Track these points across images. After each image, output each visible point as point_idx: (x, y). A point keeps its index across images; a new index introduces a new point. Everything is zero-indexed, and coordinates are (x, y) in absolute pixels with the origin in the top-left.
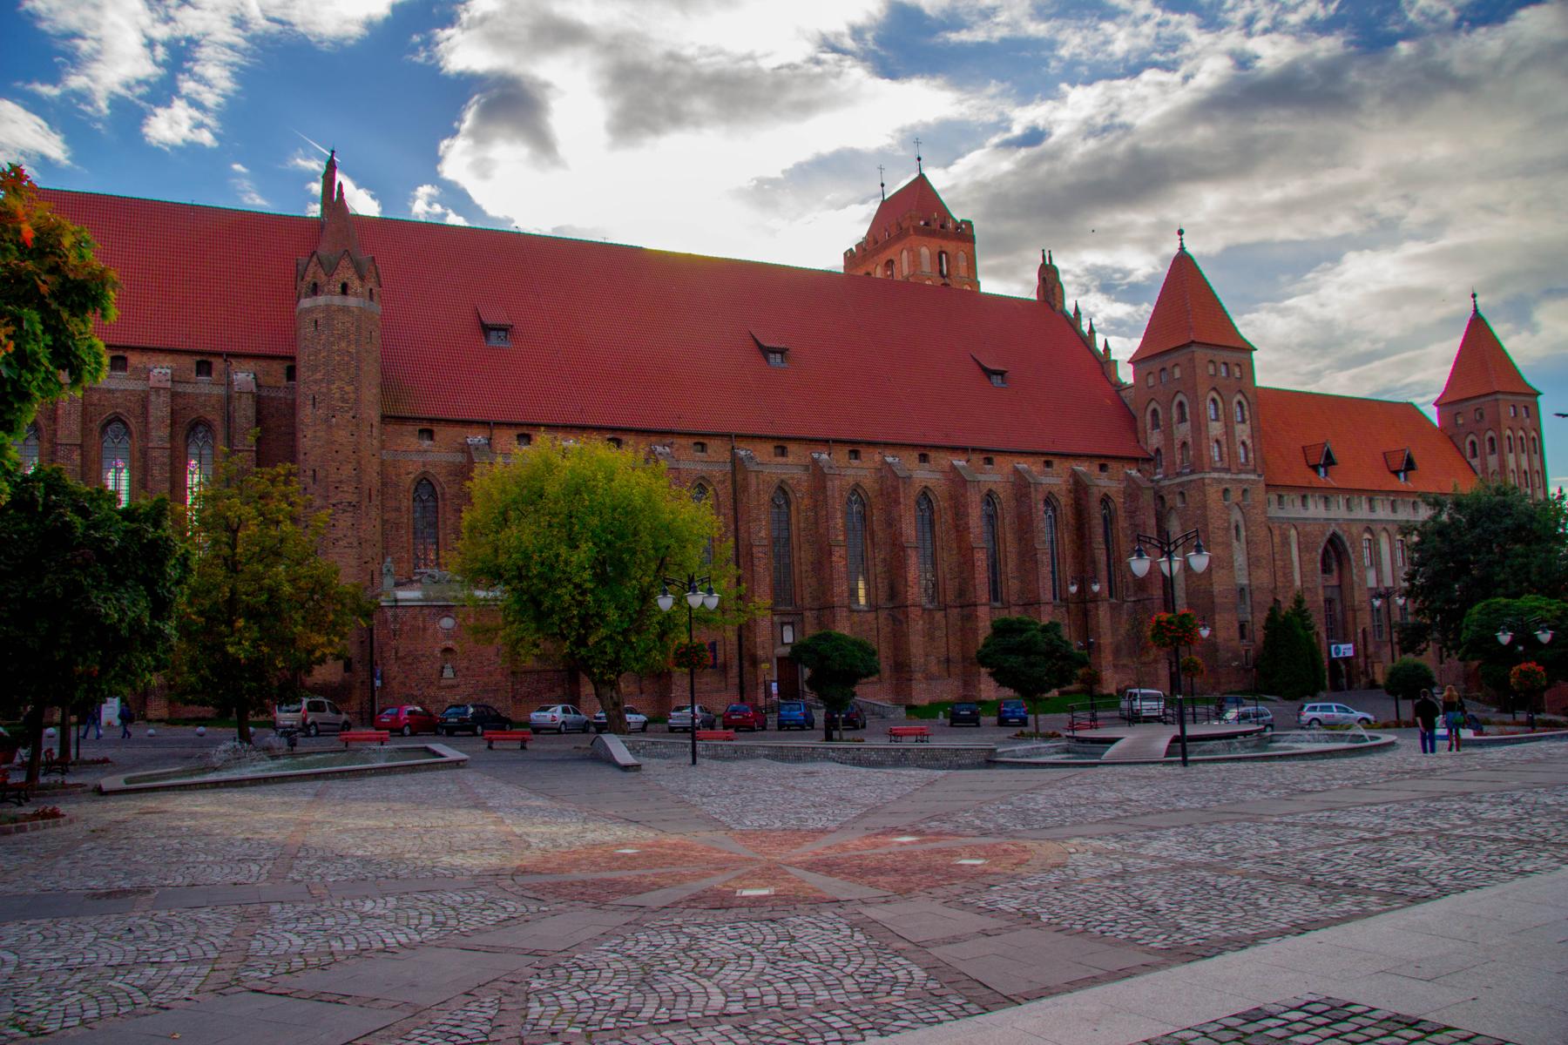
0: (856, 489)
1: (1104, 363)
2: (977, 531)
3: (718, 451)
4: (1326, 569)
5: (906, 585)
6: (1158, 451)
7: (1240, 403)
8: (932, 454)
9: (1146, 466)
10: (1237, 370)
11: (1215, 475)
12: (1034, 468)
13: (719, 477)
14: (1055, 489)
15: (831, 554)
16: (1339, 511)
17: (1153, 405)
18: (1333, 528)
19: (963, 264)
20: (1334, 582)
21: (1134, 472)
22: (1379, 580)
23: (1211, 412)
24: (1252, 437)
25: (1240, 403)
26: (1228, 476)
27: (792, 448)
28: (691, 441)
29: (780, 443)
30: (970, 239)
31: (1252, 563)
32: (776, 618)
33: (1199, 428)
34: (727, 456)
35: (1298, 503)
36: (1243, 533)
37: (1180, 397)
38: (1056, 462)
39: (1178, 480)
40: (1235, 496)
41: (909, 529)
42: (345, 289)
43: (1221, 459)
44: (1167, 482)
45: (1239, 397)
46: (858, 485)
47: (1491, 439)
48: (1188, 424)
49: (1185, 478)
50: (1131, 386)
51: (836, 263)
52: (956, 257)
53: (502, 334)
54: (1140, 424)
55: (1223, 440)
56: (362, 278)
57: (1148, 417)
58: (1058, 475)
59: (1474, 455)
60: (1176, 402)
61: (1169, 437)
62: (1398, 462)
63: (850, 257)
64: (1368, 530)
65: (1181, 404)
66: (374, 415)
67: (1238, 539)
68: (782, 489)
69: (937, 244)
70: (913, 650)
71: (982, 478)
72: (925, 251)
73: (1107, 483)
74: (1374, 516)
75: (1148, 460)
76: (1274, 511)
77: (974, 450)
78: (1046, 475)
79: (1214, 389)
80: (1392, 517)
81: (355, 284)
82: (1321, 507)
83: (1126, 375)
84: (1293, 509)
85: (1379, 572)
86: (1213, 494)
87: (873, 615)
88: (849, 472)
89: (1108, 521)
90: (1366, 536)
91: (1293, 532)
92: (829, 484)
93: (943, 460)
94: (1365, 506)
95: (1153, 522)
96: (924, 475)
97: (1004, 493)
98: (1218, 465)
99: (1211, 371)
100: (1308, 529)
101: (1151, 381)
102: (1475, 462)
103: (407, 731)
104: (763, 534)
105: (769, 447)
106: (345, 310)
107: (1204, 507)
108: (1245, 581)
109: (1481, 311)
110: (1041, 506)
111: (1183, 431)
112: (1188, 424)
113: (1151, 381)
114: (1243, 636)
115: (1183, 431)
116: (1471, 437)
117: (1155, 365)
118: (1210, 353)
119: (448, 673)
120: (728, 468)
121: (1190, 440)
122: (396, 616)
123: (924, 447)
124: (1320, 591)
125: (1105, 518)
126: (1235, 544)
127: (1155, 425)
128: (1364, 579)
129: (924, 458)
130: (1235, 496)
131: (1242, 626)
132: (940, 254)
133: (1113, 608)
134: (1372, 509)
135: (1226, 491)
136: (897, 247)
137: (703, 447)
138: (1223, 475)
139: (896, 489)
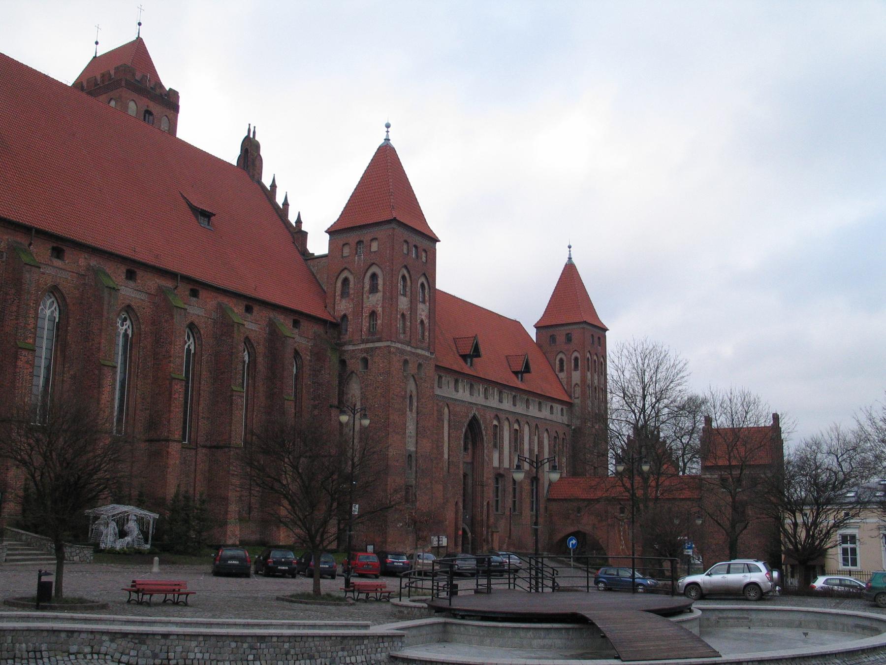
1: (298, 235)
6: (345, 316)
8: (140, 273)
10: (424, 254)
11: (399, 346)
14: (252, 336)
15: (16, 358)
16: (479, 399)
18: (474, 411)
20: (469, 460)
23: (400, 286)
25: (422, 285)
26: (409, 349)
30: (175, 108)
31: (420, 432)
35: (452, 385)
36: (415, 404)
38: (256, 309)
39: (363, 346)
40: (412, 368)
44: (351, 348)
45: (423, 279)
47: (576, 359)
48: (379, 295)
55: (408, 314)
57: (339, 284)
59: (562, 370)
60: (369, 274)
61: (360, 305)
62: (520, 367)
64: (497, 417)
65: (374, 276)
67: (411, 410)
72: (132, 105)
79: (406, 267)
80: (513, 409)
82: (467, 392)
83: (318, 244)
84: (447, 391)
85: (501, 454)
88: (49, 270)
90: (495, 423)
91: (446, 410)
94: (497, 397)
99: (405, 252)
100: (458, 409)
102: (562, 375)
108: (413, 449)
109: (574, 261)
111: (374, 301)
112: (379, 295)
115: (374, 301)
116: (561, 356)
117: (353, 238)
118: (407, 235)
124: (461, 466)
126: (408, 413)
127: (344, 294)
128: (491, 460)
129: (131, 275)
130: (412, 368)
134: (501, 401)
135: (406, 362)
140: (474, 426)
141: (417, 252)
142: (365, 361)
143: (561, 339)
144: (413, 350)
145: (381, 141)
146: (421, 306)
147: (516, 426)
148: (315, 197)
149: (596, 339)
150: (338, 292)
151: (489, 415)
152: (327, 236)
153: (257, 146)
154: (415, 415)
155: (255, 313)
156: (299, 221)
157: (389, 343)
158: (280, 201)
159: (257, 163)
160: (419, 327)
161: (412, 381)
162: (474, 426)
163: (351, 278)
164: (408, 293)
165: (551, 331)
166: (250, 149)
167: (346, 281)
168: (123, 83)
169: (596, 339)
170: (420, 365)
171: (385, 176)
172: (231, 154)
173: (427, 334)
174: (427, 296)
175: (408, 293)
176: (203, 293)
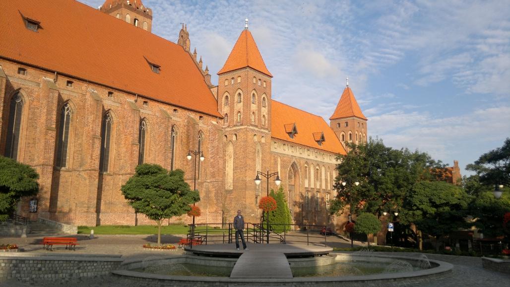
1: (205, 76)
4: (290, 178)
6: (226, 114)
8: (116, 93)
9: (220, 121)
11: (252, 128)
18: (294, 160)
22: (309, 185)
26: (256, 129)
38: (179, 110)
39: (234, 128)
49: (237, 128)
64: (306, 163)
69: (135, 15)
74: (309, 158)
75: (221, 118)
77: (139, 96)
78: (174, 116)
80: (316, 159)
83: (214, 80)
85: (309, 181)
90: (306, 165)
91: (279, 159)
98: (253, 123)
107: (246, 141)
112: (242, 103)
113: (226, 83)
117: (229, 76)
124: (288, 186)
127: (226, 104)
132: (135, 20)
140: (294, 166)
143: (343, 125)
144: (259, 130)
146: (263, 109)
147: (317, 167)
149: (361, 124)
150: (223, 103)
151: (302, 162)
155: (179, 113)
156: (207, 69)
157: (246, 127)
158: (198, 60)
159: (187, 42)
162: (294, 166)
163: (229, 96)
165: (338, 121)
166: (184, 35)
168: (123, 6)
169: (361, 124)
172: (174, 38)
175: (257, 103)
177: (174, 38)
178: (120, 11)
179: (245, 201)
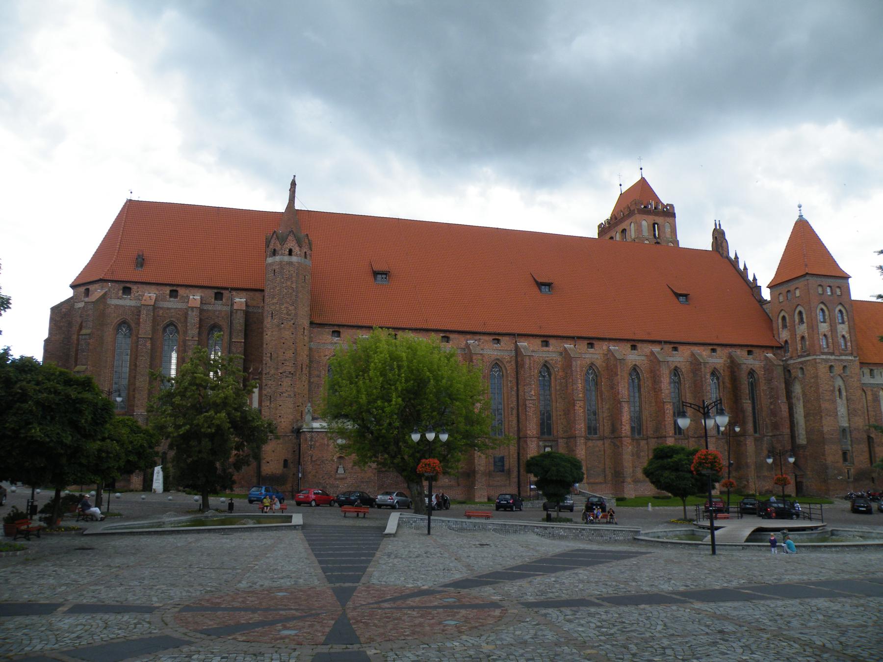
0: (591, 366)
1: (755, 288)
2: (667, 392)
3: (506, 344)
5: (621, 424)
6: (786, 342)
7: (840, 311)
8: (639, 345)
9: (779, 351)
11: (824, 357)
12: (704, 353)
13: (508, 358)
14: (718, 366)
15: (574, 406)
17: (783, 313)
19: (668, 230)
21: (770, 355)
23: (820, 317)
24: (850, 333)
25: (840, 311)
26: (833, 357)
27: (552, 341)
28: (491, 338)
29: (545, 339)
30: (673, 215)
31: (851, 413)
32: (541, 443)
33: (813, 328)
34: (512, 346)
36: (844, 394)
37: (799, 308)
38: (719, 349)
39: (800, 360)
40: (838, 370)
41: (623, 389)
42: (290, 252)
43: (828, 347)
44: (792, 362)
45: (840, 307)
46: (592, 363)
48: (805, 325)
50: (769, 302)
51: (594, 234)
52: (664, 226)
53: (384, 276)
54: (774, 325)
55: (829, 334)
56: (300, 246)
57: (780, 321)
58: (721, 358)
60: (797, 312)
61: (793, 334)
63: (603, 229)
65: (800, 313)
66: (306, 323)
68: (546, 366)
69: (652, 219)
70: (626, 464)
71: (669, 359)
72: (644, 223)
73: (749, 362)
75: (780, 348)
76: (867, 379)
77: (666, 342)
78: (712, 357)
79: (822, 303)
81: (296, 250)
83: (766, 294)
86: (823, 369)
87: (601, 442)
89: (753, 386)
92: (574, 363)
93: (647, 349)
95: (783, 386)
96: (633, 357)
97: (684, 368)
98: (826, 350)
101: (781, 299)
103: (313, 503)
104: (533, 393)
105: (538, 341)
106: (290, 264)
107: (816, 377)
110: (708, 376)
111: (802, 330)
112: (805, 325)
113: (781, 299)
114: (845, 459)
115: (802, 330)
118: (819, 281)
119: (341, 471)
120: (513, 353)
121: (806, 335)
122: (312, 437)
123: (634, 340)
125: (752, 384)
127: (784, 326)
129: (634, 347)
130: (838, 370)
131: (845, 454)
132: (654, 224)
133: (756, 440)
136: (627, 222)
137: (498, 341)
138: (829, 357)
139: (616, 366)
141: (831, 290)
142: (802, 368)
145: (796, 218)
148: (762, 262)
150: (780, 326)
152: (769, 290)
153: (723, 233)
154: (845, 402)
156: (755, 279)
159: (724, 244)
160: (842, 341)
161: (839, 378)
164: (828, 320)
166: (719, 236)
167: (784, 318)
170: (845, 367)
171: (804, 238)
172: (705, 243)
173: (849, 344)
174: (845, 318)
175: (828, 320)
176: (681, 348)
177: (705, 243)
178: (633, 219)
179: (825, 460)
